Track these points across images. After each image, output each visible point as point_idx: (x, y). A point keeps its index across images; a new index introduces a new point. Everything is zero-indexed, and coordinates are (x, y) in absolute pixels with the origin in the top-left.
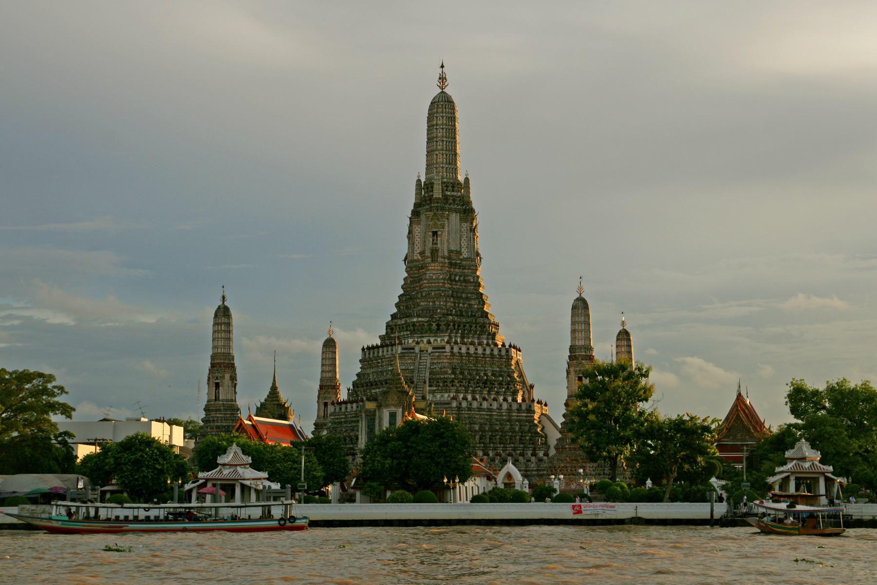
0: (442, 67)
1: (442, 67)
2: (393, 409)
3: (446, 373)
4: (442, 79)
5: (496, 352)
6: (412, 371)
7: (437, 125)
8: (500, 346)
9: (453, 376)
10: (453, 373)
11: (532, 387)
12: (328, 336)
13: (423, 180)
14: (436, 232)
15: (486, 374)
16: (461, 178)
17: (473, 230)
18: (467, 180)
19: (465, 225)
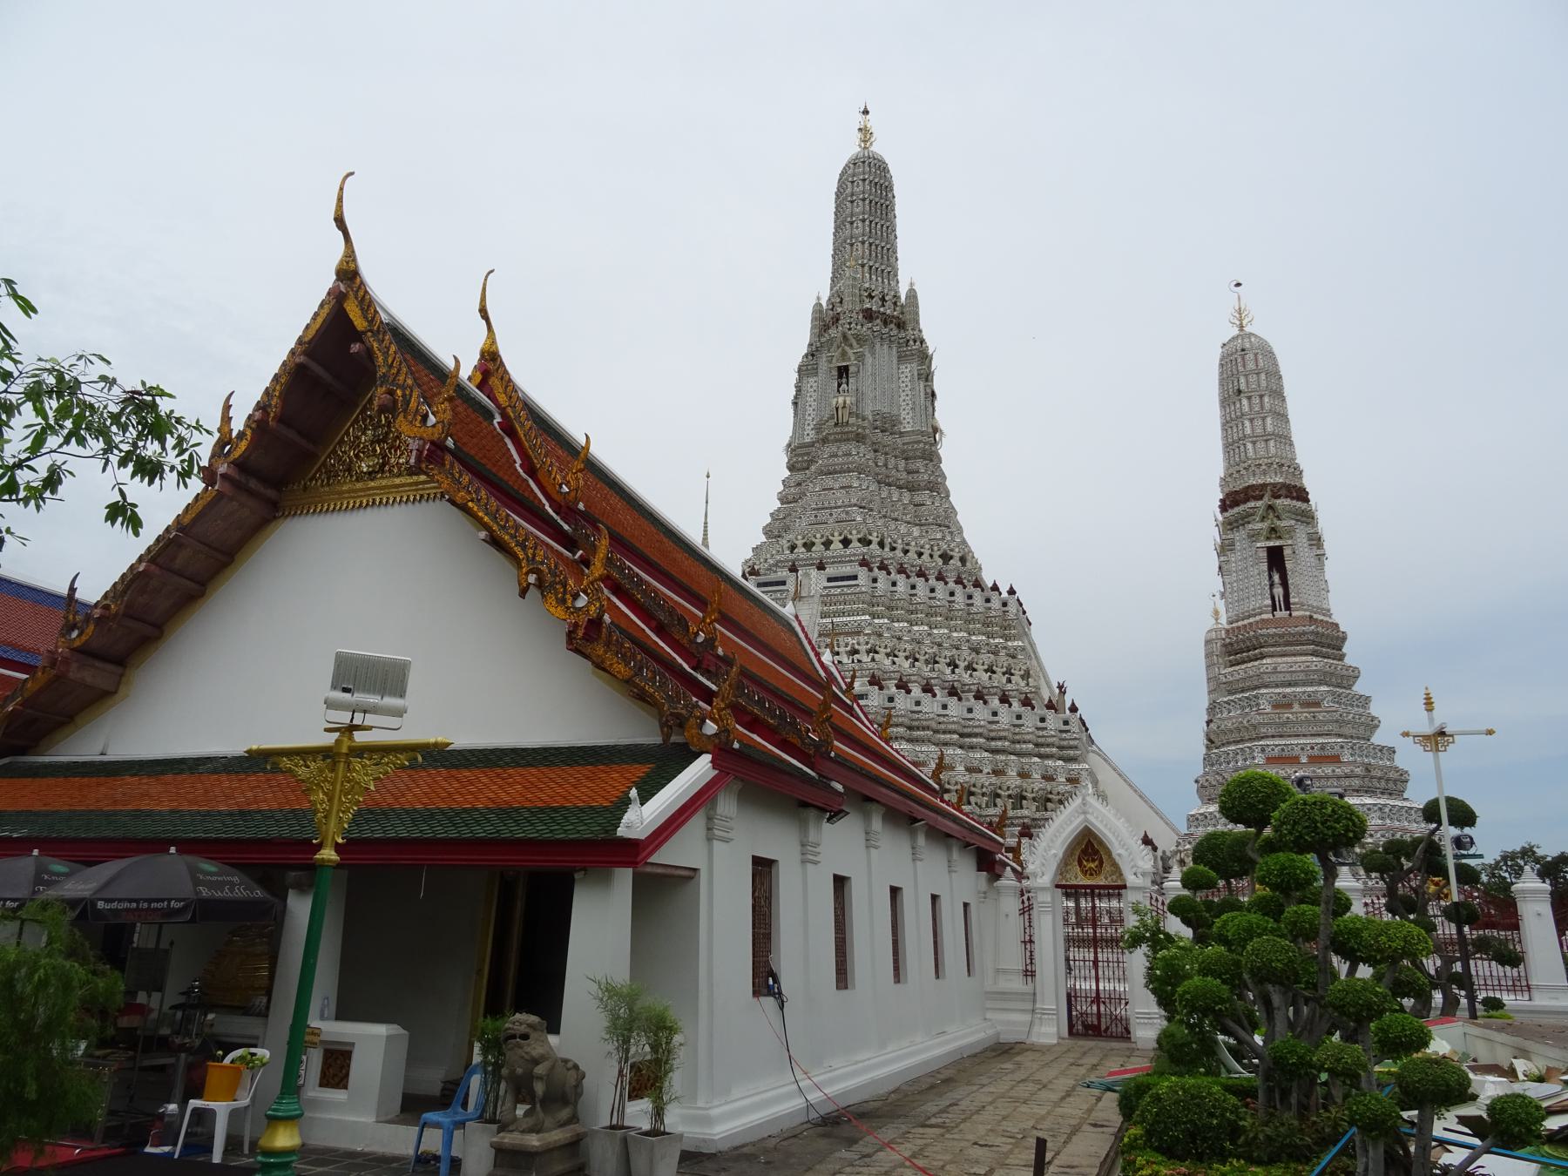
0: (866, 112)
1: (866, 112)
4: (865, 132)
14: (846, 368)
18: (912, 295)
19: (909, 370)
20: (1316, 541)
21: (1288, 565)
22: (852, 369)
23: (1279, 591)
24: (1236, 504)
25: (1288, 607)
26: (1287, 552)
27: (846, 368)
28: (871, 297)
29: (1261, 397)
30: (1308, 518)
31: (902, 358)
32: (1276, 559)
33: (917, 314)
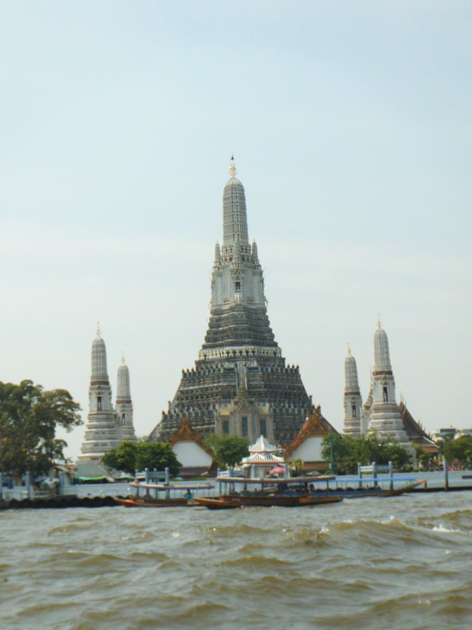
0: (233, 159)
1: (233, 159)
2: (244, 415)
3: (260, 387)
5: (289, 372)
6: (234, 387)
7: (232, 203)
8: (291, 367)
9: (266, 390)
10: (265, 387)
11: (311, 397)
12: (122, 364)
13: (221, 244)
14: (239, 283)
15: (285, 389)
16: (251, 242)
17: (262, 281)
19: (256, 279)
20: (394, 384)
21: (388, 391)
22: (241, 284)
23: (385, 397)
24: (377, 374)
25: (387, 400)
26: (388, 388)
27: (239, 283)
28: (242, 249)
29: (384, 349)
30: (392, 378)
31: (254, 274)
32: (385, 390)
33: (257, 253)
